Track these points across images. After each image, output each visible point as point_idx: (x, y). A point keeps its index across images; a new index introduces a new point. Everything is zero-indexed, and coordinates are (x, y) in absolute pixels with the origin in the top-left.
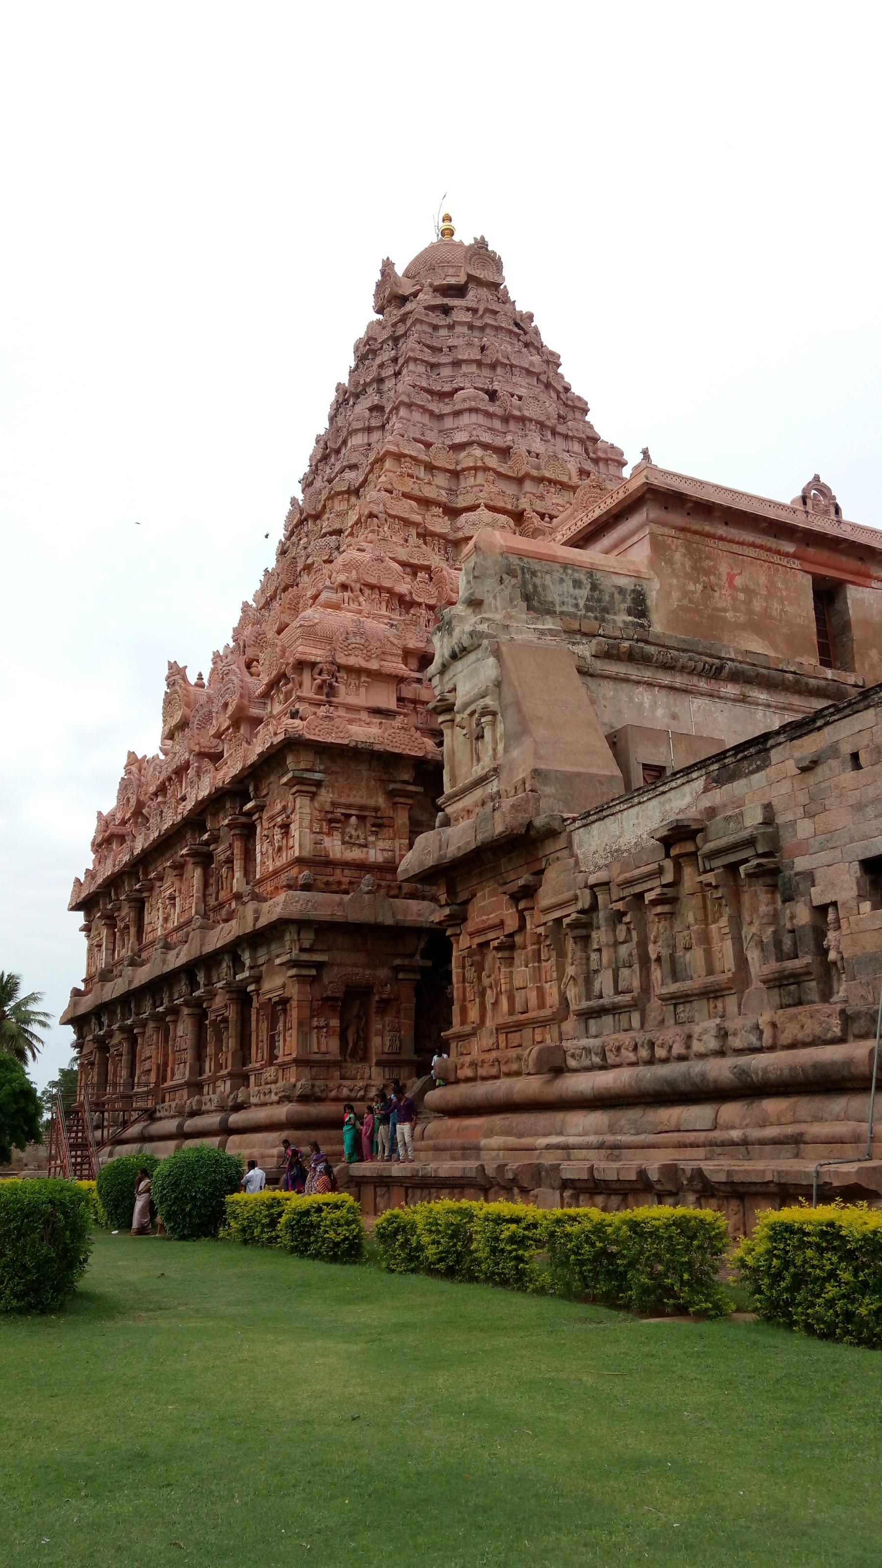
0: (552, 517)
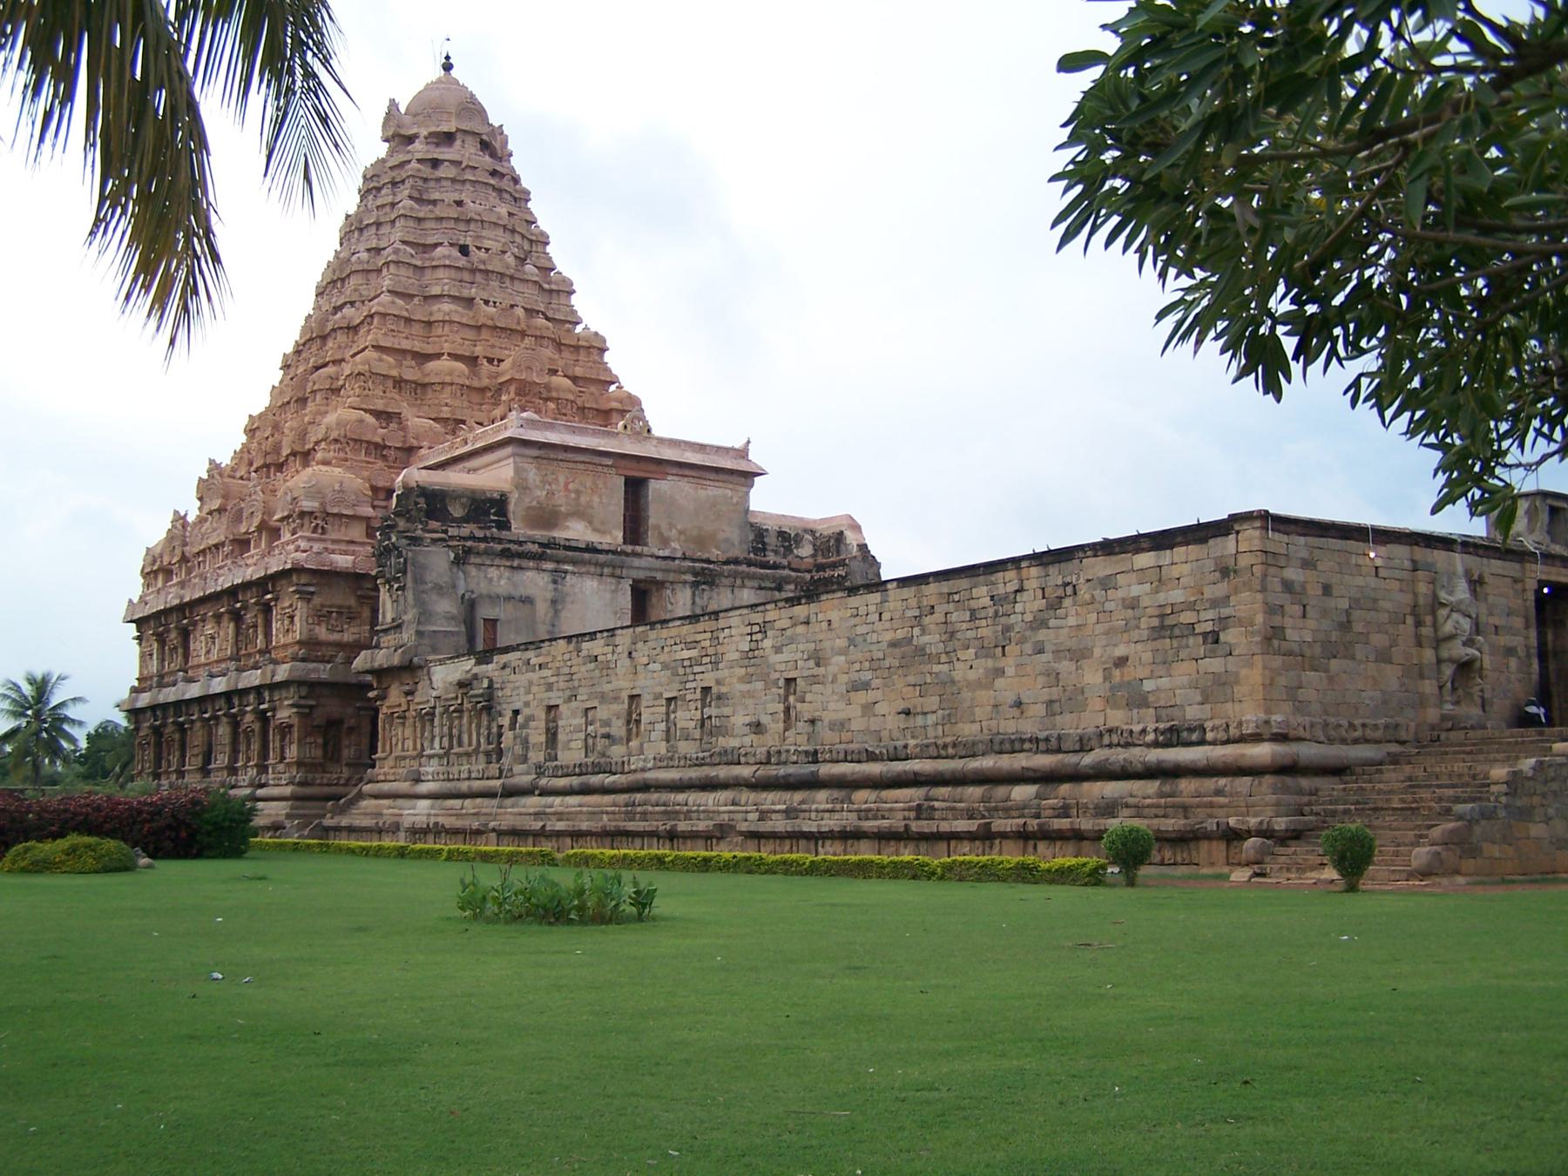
0: (500, 361)
